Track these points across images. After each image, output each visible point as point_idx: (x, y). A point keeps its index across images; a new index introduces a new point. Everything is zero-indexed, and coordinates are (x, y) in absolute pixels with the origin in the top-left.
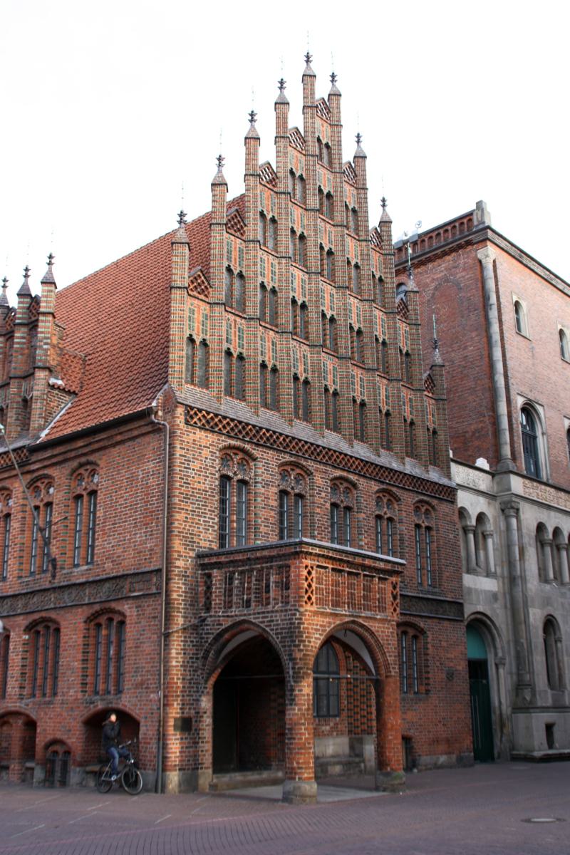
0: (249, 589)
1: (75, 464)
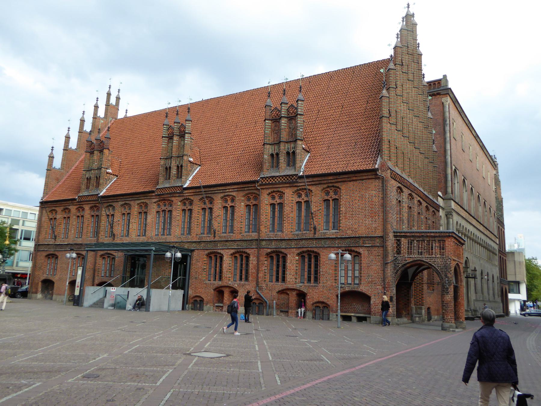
0: (422, 247)
1: (325, 186)
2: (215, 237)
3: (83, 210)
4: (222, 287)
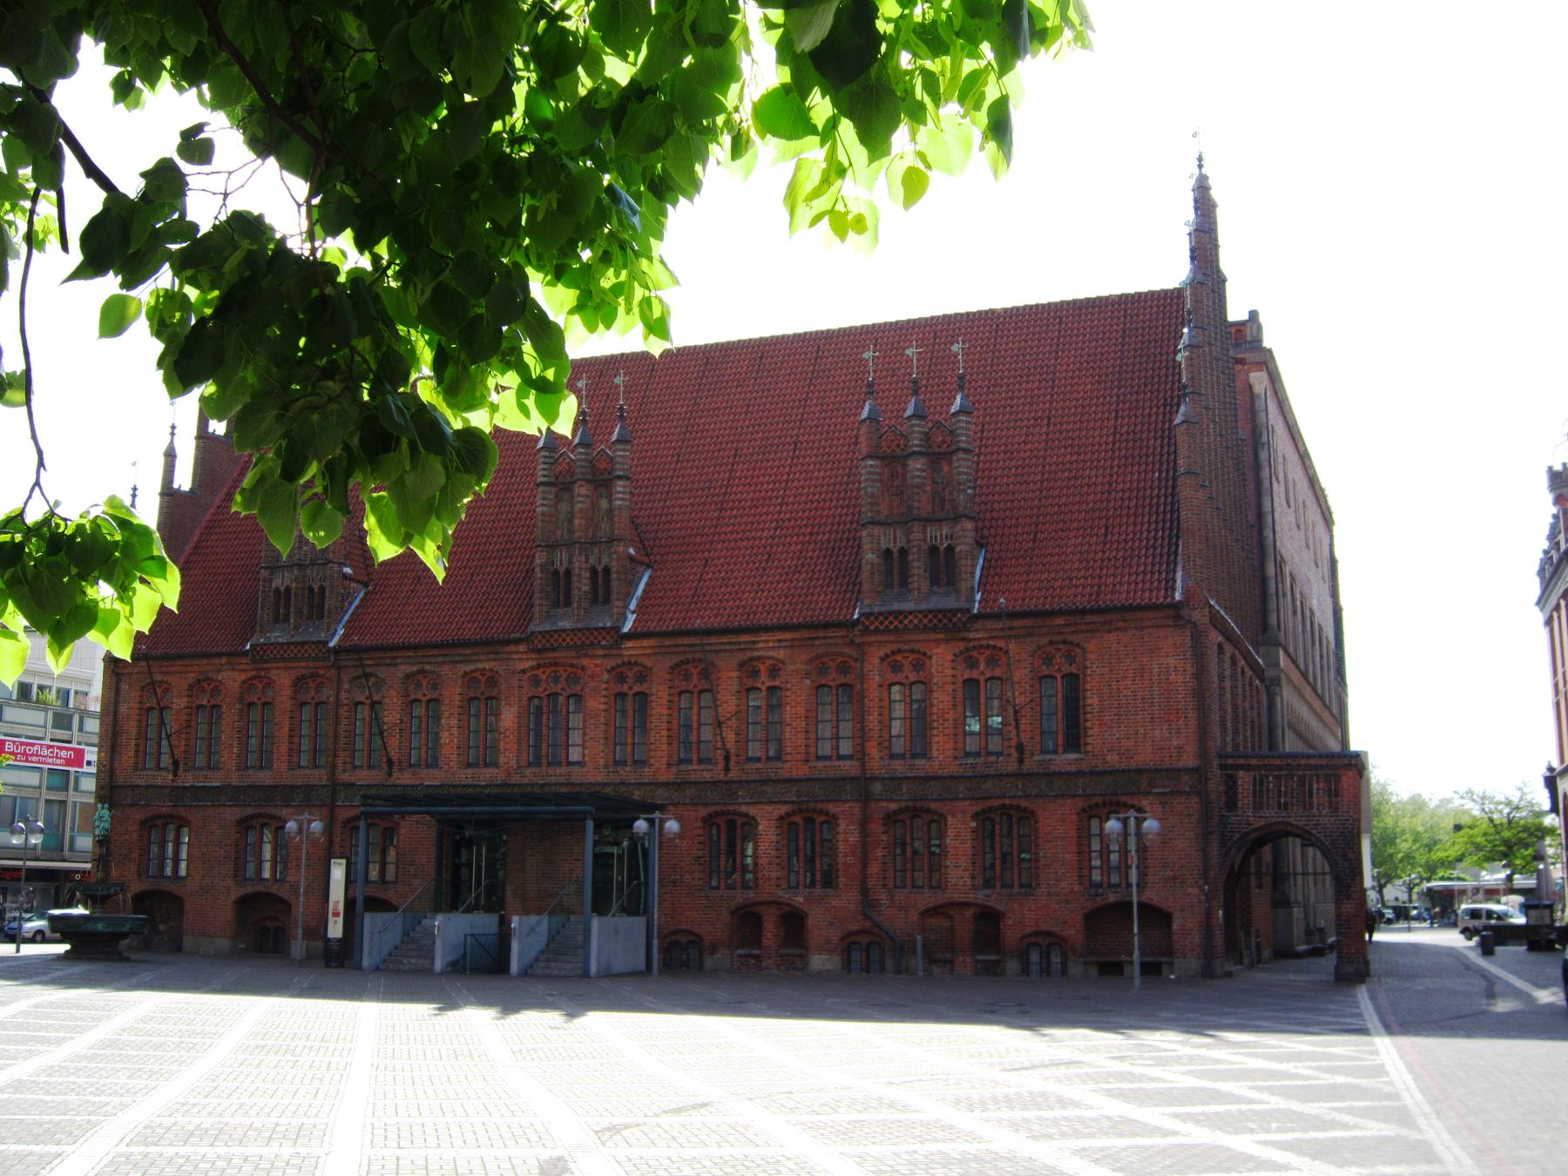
3: (269, 684)
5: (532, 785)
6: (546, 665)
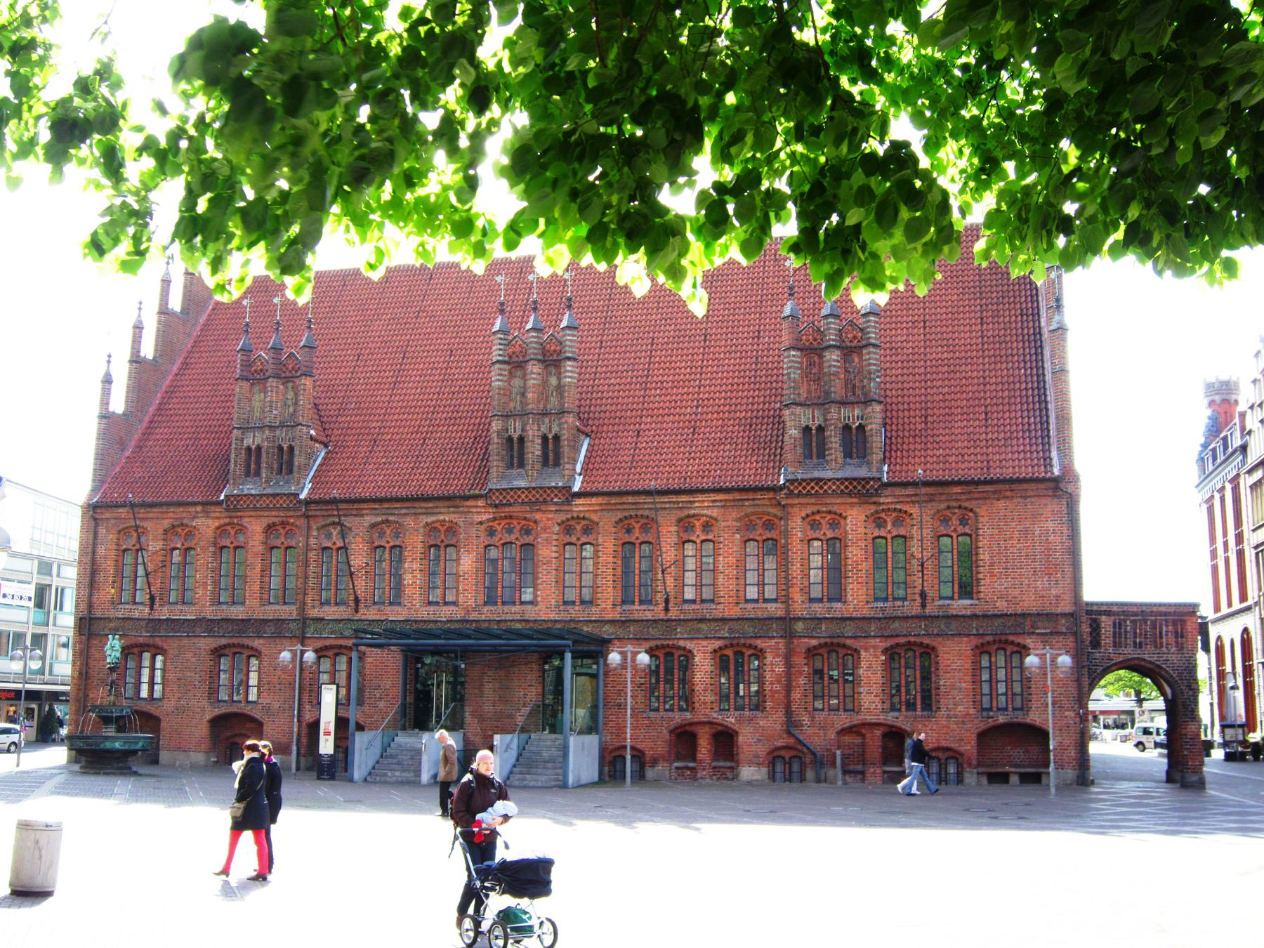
2: (667, 610)
4: (691, 724)
5: (489, 621)
6: (501, 519)
